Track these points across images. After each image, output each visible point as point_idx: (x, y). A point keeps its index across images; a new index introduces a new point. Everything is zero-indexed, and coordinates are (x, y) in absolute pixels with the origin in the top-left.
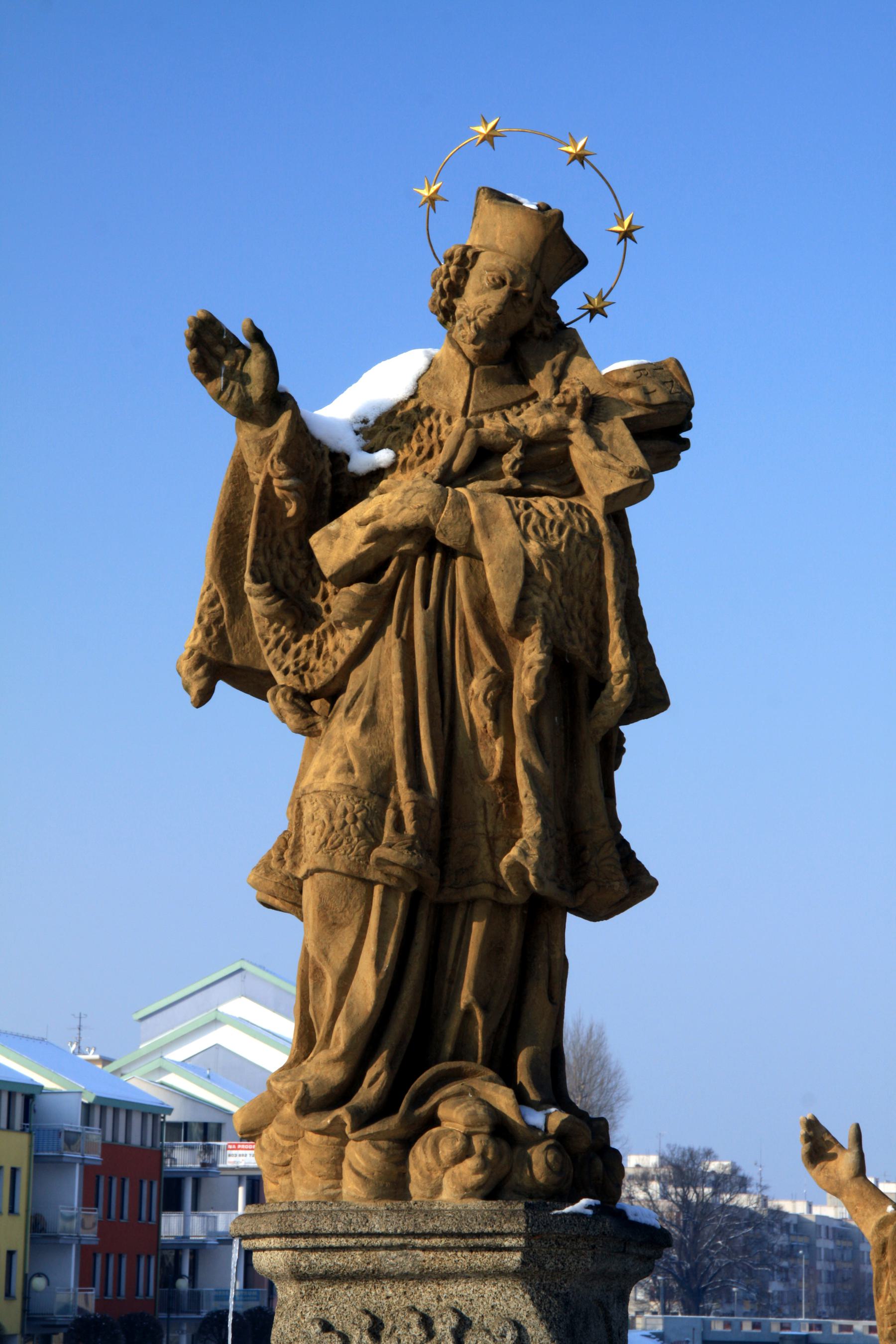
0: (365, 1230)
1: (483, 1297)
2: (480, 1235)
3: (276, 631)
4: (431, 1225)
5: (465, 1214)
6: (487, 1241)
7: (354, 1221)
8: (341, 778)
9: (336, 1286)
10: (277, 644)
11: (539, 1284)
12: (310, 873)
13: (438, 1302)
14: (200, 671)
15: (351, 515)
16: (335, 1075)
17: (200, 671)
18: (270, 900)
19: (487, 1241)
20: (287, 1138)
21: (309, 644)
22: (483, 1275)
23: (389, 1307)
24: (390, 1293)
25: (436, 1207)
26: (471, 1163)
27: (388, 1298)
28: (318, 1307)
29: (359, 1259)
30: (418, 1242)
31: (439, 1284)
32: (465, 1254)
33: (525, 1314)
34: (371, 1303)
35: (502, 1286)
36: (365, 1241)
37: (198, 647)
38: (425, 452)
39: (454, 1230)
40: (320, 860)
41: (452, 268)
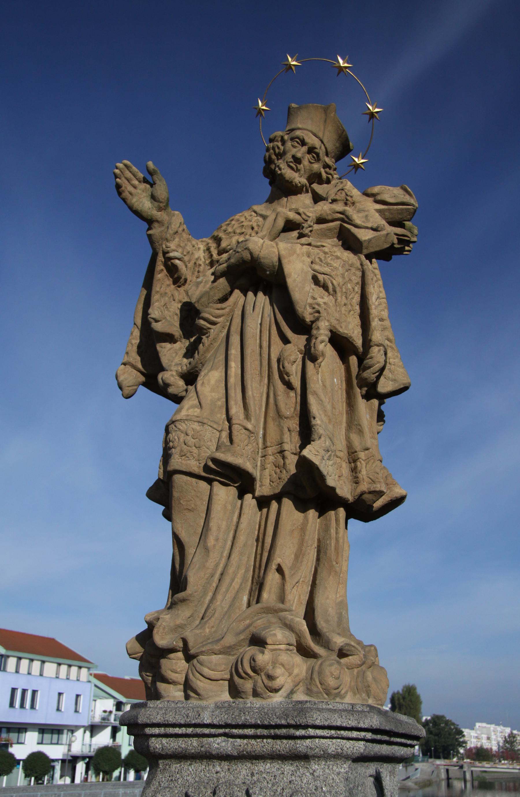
1: (283, 773)
4: (243, 718)
5: (268, 711)
6: (284, 731)
7: (190, 714)
9: (182, 763)
11: (325, 764)
13: (252, 778)
19: (284, 731)
23: (218, 780)
24: (218, 769)
25: (249, 705)
27: (217, 773)
28: (170, 779)
31: (252, 764)
32: (269, 740)
33: (314, 787)
34: (205, 776)
35: (297, 766)
36: (199, 730)
39: (259, 722)
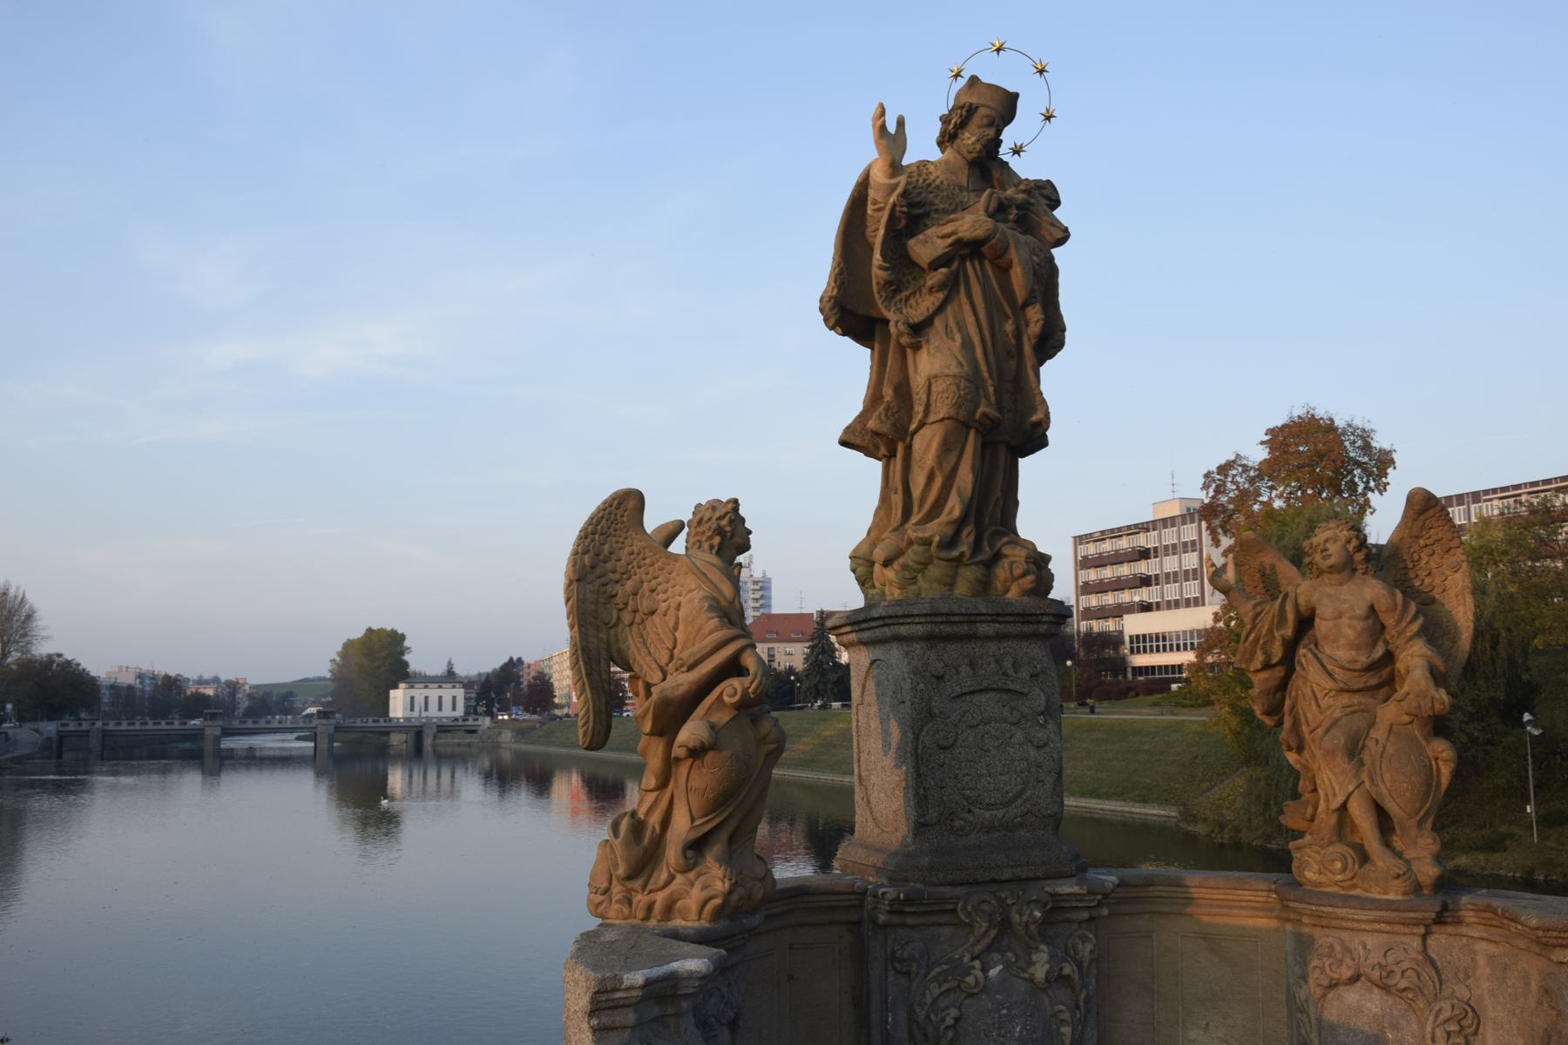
0: (976, 612)
2: (1030, 615)
3: (886, 291)
8: (960, 370)
10: (886, 297)
12: (942, 420)
14: (836, 310)
15: (932, 232)
16: (950, 530)
17: (836, 310)
18: (852, 440)
20: (921, 564)
21: (901, 300)
22: (1023, 637)
24: (974, 646)
26: (1030, 578)
29: (966, 628)
30: (1000, 619)
32: (1020, 625)
36: (973, 618)
37: (835, 297)
38: (953, 207)
40: (952, 413)
41: (964, 113)
